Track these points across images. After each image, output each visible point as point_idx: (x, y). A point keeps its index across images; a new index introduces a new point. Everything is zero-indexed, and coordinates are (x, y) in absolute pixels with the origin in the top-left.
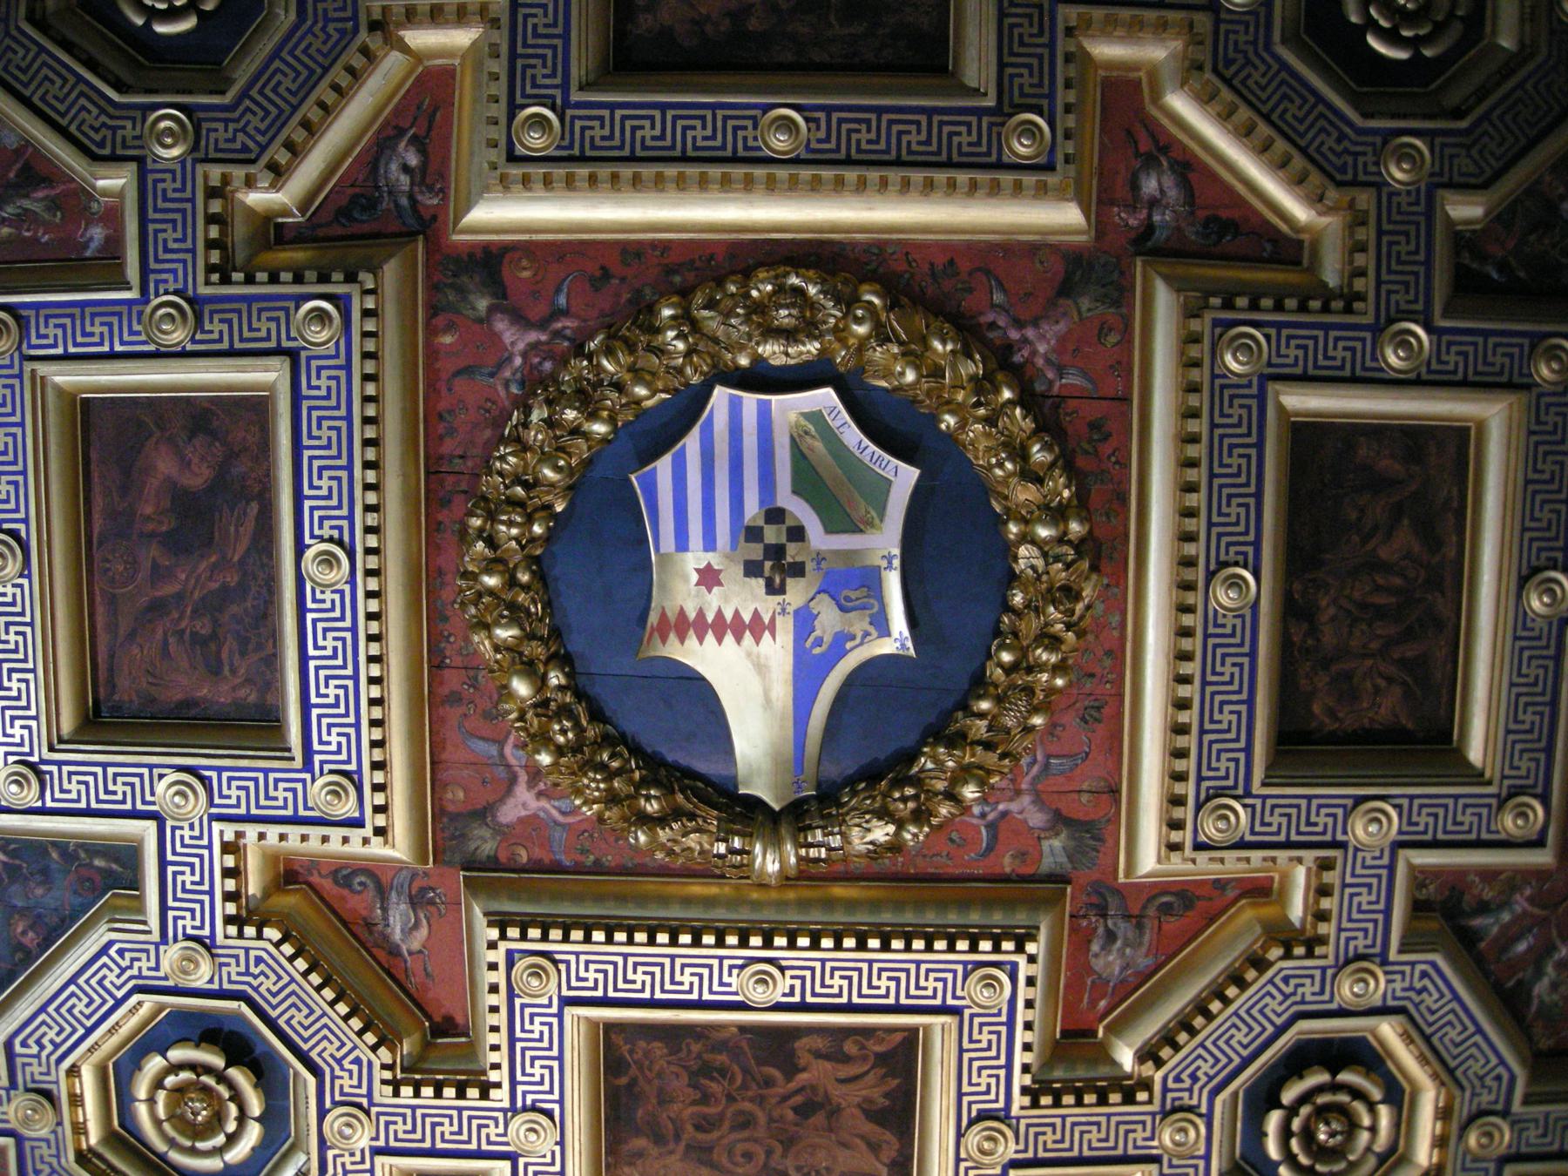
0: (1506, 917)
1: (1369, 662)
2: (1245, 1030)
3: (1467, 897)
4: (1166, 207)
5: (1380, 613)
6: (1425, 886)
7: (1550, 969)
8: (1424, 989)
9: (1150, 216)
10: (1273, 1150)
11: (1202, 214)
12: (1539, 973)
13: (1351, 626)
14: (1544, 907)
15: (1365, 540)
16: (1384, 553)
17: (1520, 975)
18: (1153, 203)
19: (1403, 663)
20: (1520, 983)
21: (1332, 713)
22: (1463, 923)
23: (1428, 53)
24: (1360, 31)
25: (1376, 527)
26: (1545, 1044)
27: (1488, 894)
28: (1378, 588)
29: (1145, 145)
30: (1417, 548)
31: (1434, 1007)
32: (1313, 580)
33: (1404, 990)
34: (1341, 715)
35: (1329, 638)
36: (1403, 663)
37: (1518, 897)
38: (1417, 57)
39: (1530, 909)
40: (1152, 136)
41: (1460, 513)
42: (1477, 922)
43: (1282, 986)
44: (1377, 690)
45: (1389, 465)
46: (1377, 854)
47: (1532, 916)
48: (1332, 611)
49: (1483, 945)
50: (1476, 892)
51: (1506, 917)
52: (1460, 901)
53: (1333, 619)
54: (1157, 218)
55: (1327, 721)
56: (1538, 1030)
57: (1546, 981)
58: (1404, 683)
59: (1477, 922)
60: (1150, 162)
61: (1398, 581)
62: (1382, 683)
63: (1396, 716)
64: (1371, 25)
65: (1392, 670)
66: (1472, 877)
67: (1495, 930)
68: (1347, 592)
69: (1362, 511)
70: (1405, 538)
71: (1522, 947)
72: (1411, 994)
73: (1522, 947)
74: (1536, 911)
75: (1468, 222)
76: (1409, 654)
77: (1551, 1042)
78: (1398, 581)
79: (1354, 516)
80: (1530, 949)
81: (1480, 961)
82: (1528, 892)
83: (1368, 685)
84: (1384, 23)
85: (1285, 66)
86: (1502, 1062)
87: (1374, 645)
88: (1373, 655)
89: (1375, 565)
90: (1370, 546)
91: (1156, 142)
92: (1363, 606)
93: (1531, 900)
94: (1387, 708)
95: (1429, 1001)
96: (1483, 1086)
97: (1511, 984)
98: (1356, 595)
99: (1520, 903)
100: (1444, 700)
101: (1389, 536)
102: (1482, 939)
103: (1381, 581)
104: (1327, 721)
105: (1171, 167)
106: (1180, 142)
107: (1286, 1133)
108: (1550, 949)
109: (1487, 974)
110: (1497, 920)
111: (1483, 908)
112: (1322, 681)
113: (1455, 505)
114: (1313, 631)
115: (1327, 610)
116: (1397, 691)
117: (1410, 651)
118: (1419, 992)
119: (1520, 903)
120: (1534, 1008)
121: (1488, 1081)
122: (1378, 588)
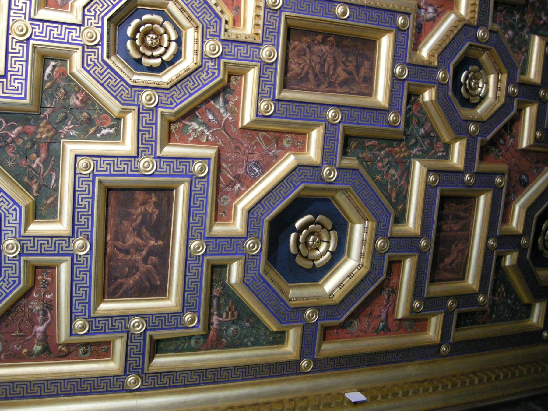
0: (222, 111)
1: (308, 62)
2: (198, 6)
3: (230, 96)
4: (425, 14)
5: (323, 66)
6: (236, 80)
7: (201, 128)
8: (208, 74)
9: (423, 9)
10: (146, 17)
11: (423, 23)
12: (201, 124)
13: (319, 56)
14: (224, 125)
15: (344, 63)
16: (339, 69)
17: (200, 117)
18: (426, 10)
19: (308, 73)
20: (198, 117)
21: (294, 48)
22: (221, 94)
23: (462, 89)
24: (467, 69)
25: (346, 66)
26: (173, 128)
27: (230, 103)
28: (329, 66)
29: (440, 10)
30: (340, 79)
31: (201, 78)
32: (333, 45)
33: (208, 66)
34: (293, 51)
35: (316, 48)
36: (308, 73)
37: (229, 115)
38: (461, 85)
39: (224, 120)
40: (441, 12)
41: (349, 93)
42: (221, 99)
43: (213, 20)
44: (300, 64)
45: (363, 72)
46: (257, 56)
47: (222, 120)
48: (324, 50)
49: (212, 102)
50: (232, 99)
51: (222, 111)
52: (229, 93)
53: (322, 50)
54: (422, 11)
55: (292, 46)
56: (178, 125)
57: (197, 127)
58: (301, 74)
59: (221, 99)
60: (436, 11)
61: (331, 73)
62: (302, 66)
63: (292, 70)
64: (469, 73)
65: (306, 69)
66: (237, 97)
67: (218, 107)
68: (329, 56)
69: (351, 62)
70: (343, 75)
71: (211, 117)
72: (206, 69)
73: (211, 117)
74: (223, 122)
75: (423, 98)
76: (310, 75)
77: (173, 131)
78: (331, 73)
79: (350, 59)
80: (209, 120)
81: (206, 101)
82: (230, 118)
83: (302, 61)
84: (470, 76)
85: (464, 44)
86: (177, 105)
87: (313, 64)
88: (310, 63)
89: (336, 65)
90: (341, 63)
91: (440, 13)
92: (325, 61)
93: (228, 119)
94: (294, 68)
95: (203, 75)
96: (169, 97)
97: (197, 114)
98: (328, 59)
99: (226, 116)
100: (296, 87)
101: (345, 70)
102: (215, 102)
103: (331, 67)
104: (292, 46)
105: (434, 17)
106: (440, 20)
107: (153, 22)
108: (209, 128)
109: (202, 104)
110: (221, 107)
111: (226, 102)
112: (304, 46)
113: (352, 92)
114: (319, 43)
115: (325, 48)
116: (299, 72)
117: (311, 76)
118: (207, 72)
119: (226, 116)
120: (187, 123)
121: (170, 99)
122: (329, 66)
